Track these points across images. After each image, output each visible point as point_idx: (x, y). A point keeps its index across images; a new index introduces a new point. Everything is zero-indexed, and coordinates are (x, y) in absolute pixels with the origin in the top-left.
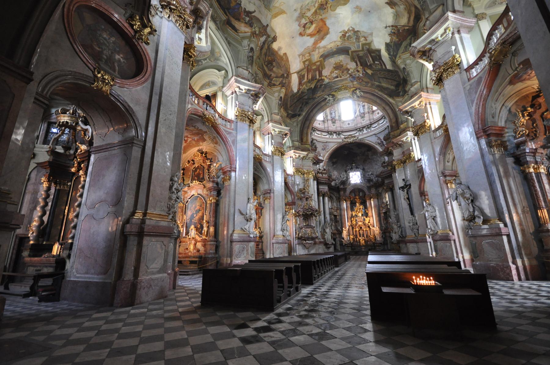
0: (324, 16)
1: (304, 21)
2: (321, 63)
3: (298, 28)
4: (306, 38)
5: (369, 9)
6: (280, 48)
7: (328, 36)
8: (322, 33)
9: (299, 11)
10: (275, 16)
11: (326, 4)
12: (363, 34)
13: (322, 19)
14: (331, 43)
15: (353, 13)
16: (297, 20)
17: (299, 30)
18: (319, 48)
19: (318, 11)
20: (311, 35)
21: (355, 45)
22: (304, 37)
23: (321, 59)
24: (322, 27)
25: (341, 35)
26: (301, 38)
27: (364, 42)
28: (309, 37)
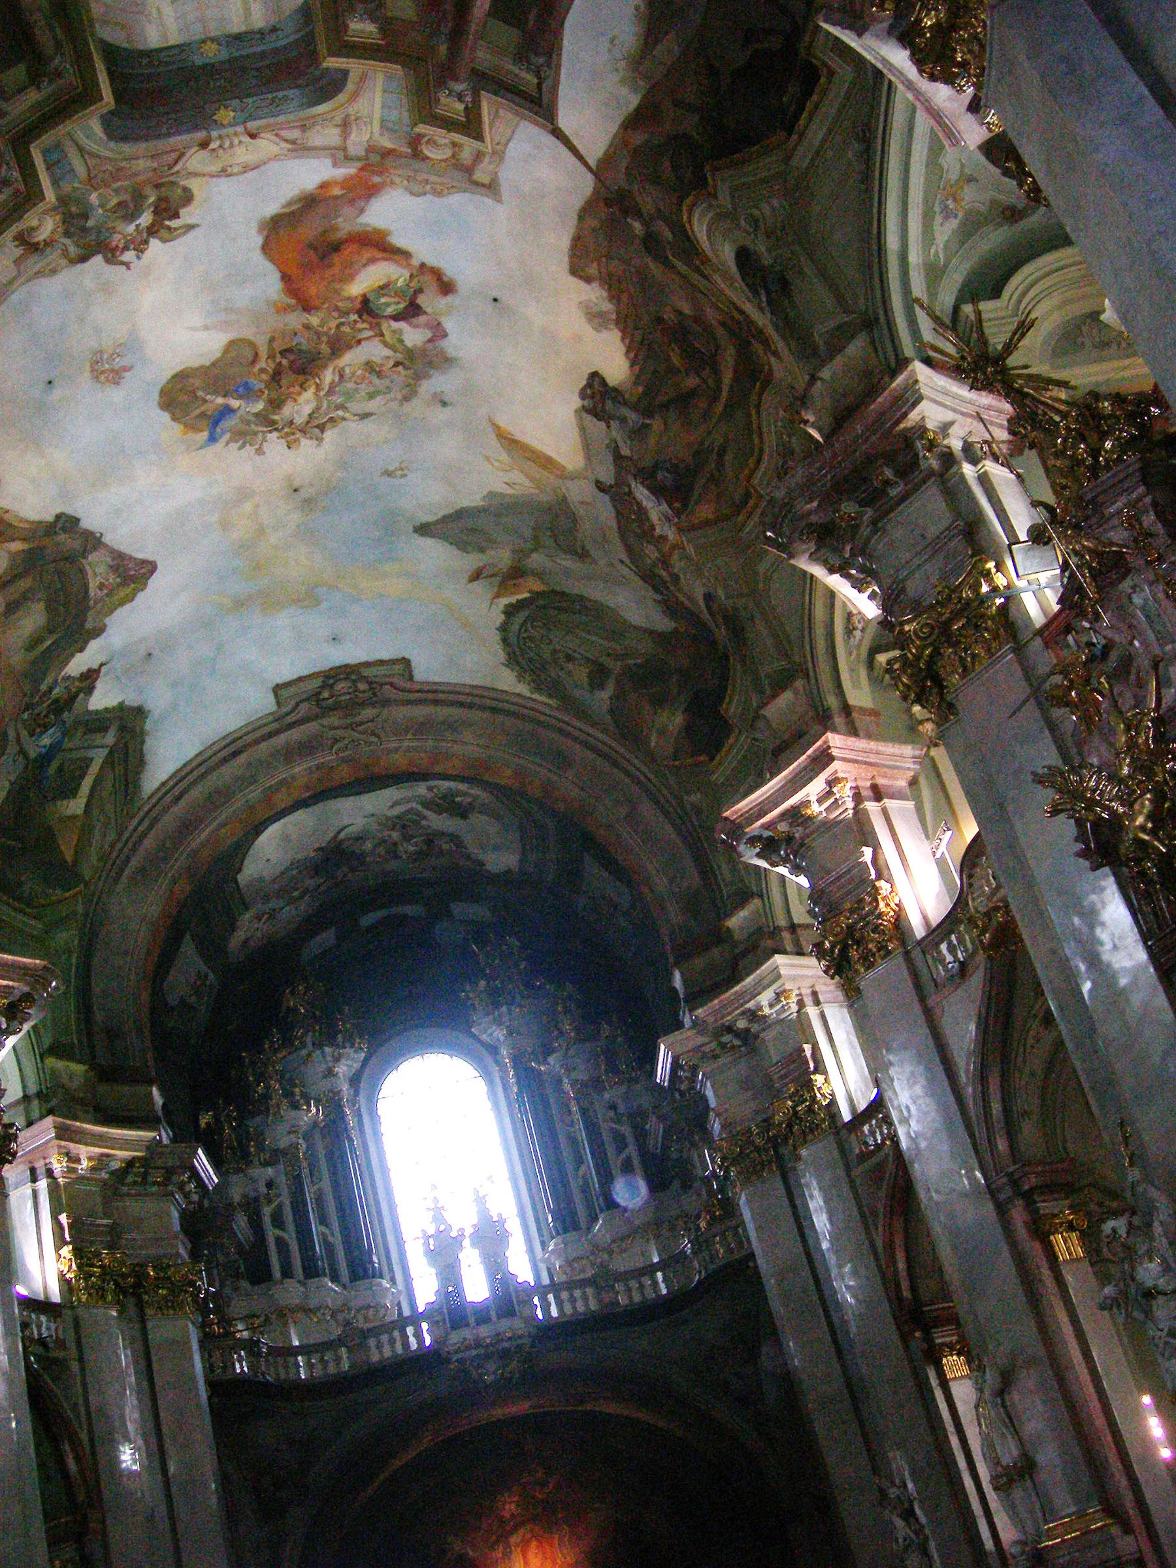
0: (295, 320)
1: (413, 335)
2: (338, 28)
3: (448, 324)
4: (424, 251)
5: (57, 394)
6: (596, 318)
7: (272, 209)
8: (309, 230)
9: (427, 387)
10: (546, 462)
11: (276, 376)
12: (53, 256)
13: (308, 308)
14: (247, 168)
15: (132, 344)
16: (446, 361)
17: (450, 310)
18: (340, 154)
19: (325, 349)
20: (378, 245)
21: (80, 169)
22: (431, 261)
23: (332, 63)
24: (308, 268)
25: (187, 215)
26: (450, 270)
27: (31, 219)
28: (398, 241)
